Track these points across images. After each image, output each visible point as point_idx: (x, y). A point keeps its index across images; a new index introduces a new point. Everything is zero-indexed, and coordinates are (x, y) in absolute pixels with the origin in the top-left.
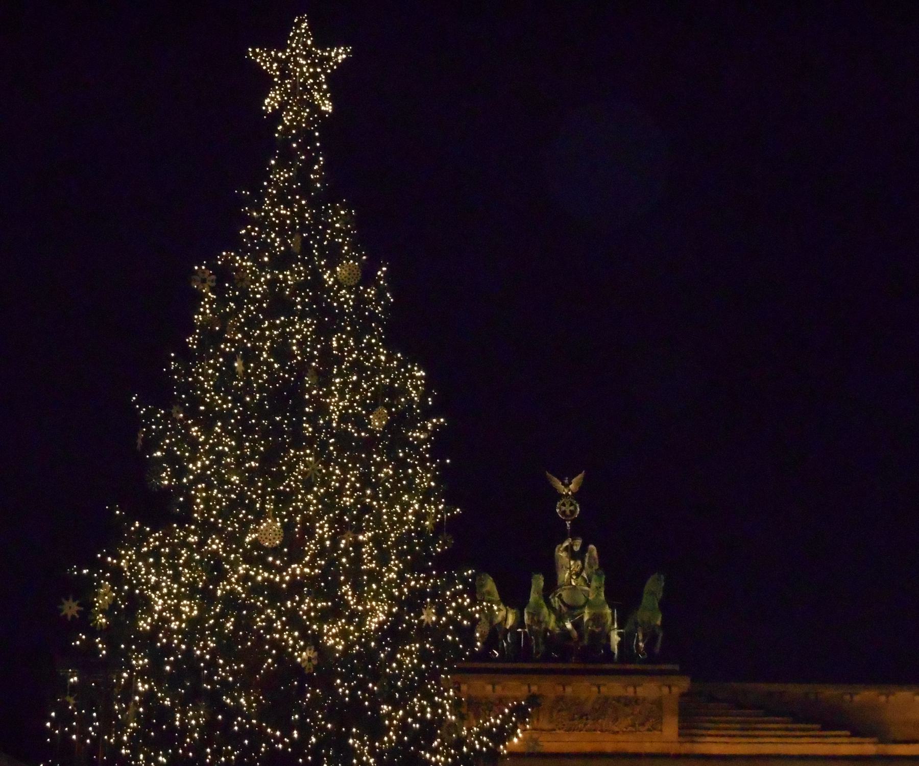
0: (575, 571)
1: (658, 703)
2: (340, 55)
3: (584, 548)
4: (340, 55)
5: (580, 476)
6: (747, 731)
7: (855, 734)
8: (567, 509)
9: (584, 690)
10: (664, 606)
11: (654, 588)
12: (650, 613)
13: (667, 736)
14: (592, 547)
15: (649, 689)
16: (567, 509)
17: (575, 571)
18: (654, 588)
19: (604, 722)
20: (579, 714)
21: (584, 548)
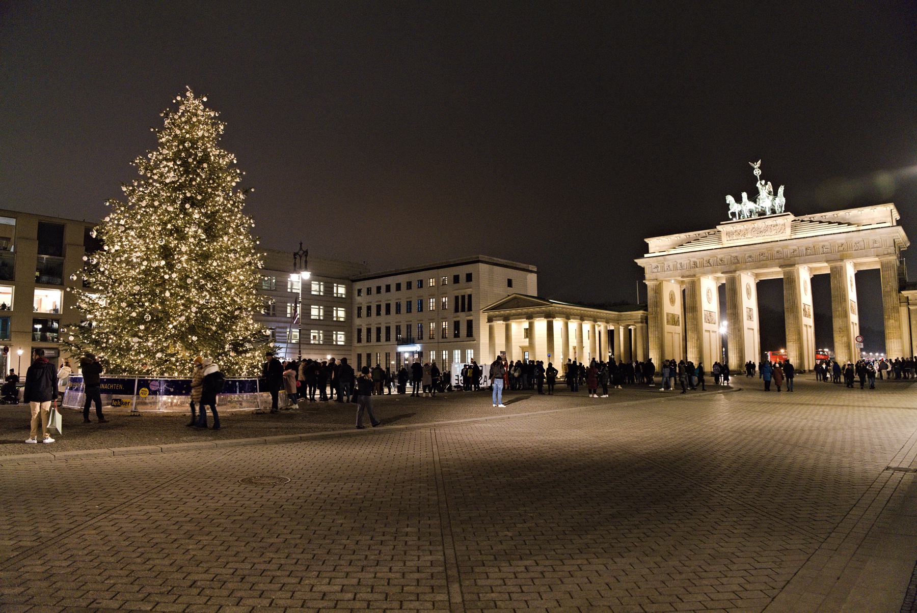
0: (764, 189)
1: (784, 225)
5: (759, 162)
6: (813, 229)
7: (849, 224)
8: (757, 172)
9: (760, 224)
11: (781, 190)
13: (787, 234)
14: (769, 183)
15: (780, 221)
16: (757, 172)
17: (764, 189)
18: (781, 190)
19: (767, 233)
20: (760, 232)
21: (766, 184)
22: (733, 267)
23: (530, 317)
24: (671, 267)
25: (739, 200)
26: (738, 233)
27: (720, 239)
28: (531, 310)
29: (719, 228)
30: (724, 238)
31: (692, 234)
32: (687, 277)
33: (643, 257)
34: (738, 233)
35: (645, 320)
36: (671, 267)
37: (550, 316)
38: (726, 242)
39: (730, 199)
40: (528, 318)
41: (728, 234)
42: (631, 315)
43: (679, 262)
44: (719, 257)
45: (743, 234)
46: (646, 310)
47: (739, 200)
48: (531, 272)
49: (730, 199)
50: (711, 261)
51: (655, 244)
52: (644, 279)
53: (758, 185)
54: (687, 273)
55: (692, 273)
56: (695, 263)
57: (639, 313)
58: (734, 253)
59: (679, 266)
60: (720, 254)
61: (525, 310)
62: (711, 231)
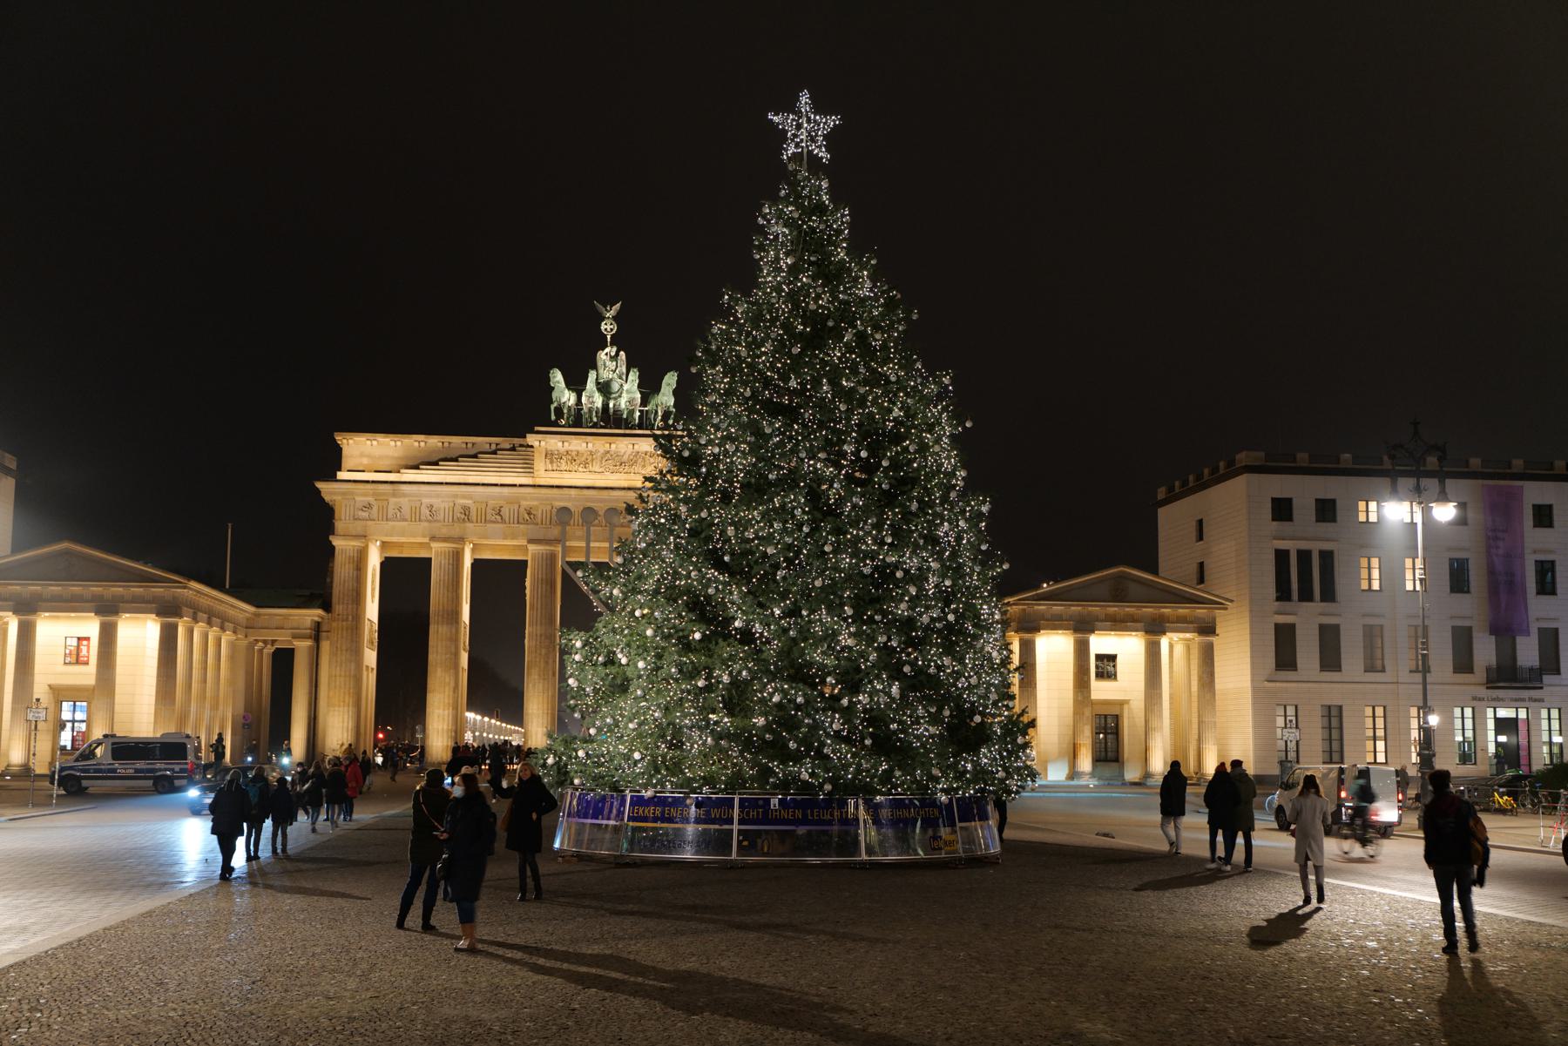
2: (805, 98)
3: (617, 354)
4: (805, 98)
8: (608, 327)
10: (675, 393)
12: (666, 398)
16: (608, 327)
21: (617, 354)
22: (555, 532)
23: (108, 610)
24: (406, 510)
25: (576, 383)
26: (573, 458)
27: (528, 466)
28: (117, 590)
29: (531, 439)
30: (540, 464)
31: (457, 441)
32: (445, 540)
33: (332, 477)
34: (573, 458)
35: (317, 633)
36: (406, 510)
37: (168, 610)
38: (544, 474)
39: (557, 377)
40: (98, 612)
41: (549, 455)
42: (286, 617)
43: (425, 501)
44: (525, 504)
45: (585, 462)
46: (327, 607)
47: (576, 383)
48: (8, 471)
49: (557, 377)
50: (505, 512)
51: (366, 454)
52: (329, 528)
53: (602, 356)
54: (444, 532)
55: (456, 531)
56: (466, 511)
57: (315, 614)
58: (561, 500)
59: (425, 512)
60: (530, 499)
61: (96, 589)
62: (505, 442)
